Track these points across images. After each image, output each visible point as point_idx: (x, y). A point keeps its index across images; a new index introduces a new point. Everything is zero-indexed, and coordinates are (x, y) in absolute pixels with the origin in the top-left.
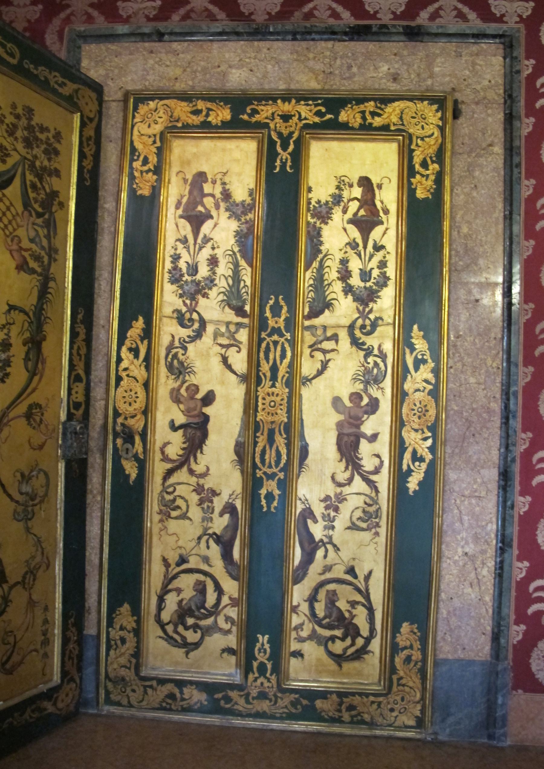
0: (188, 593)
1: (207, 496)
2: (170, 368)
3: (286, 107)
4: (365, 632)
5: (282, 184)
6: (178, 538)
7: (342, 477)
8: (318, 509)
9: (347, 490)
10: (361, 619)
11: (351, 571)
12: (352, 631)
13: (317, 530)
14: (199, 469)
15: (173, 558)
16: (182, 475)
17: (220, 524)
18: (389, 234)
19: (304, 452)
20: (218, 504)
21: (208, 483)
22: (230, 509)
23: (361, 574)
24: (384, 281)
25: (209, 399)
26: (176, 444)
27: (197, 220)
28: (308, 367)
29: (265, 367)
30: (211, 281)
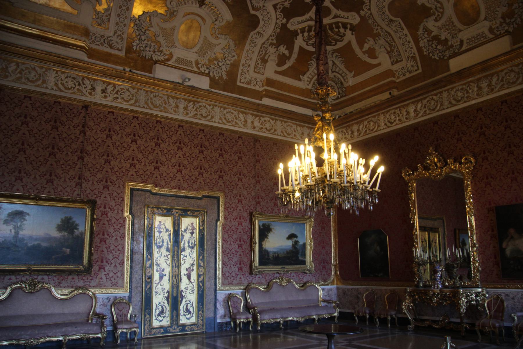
0: (161, 309)
1: (163, 289)
2: (156, 265)
3: (177, 211)
4: (192, 312)
5: (177, 225)
6: (159, 299)
7: (188, 283)
8: (184, 290)
9: (189, 286)
10: (191, 310)
11: (190, 301)
12: (190, 312)
13: (184, 294)
14: (162, 284)
15: (158, 303)
16: (159, 286)
17: (166, 295)
18: (196, 235)
19: (181, 280)
20: (166, 291)
21: (164, 287)
22: (168, 292)
23: (191, 302)
24: (195, 245)
25: (163, 270)
26: (158, 281)
27: (160, 232)
28: (182, 262)
29: (174, 264)
30: (163, 245)
